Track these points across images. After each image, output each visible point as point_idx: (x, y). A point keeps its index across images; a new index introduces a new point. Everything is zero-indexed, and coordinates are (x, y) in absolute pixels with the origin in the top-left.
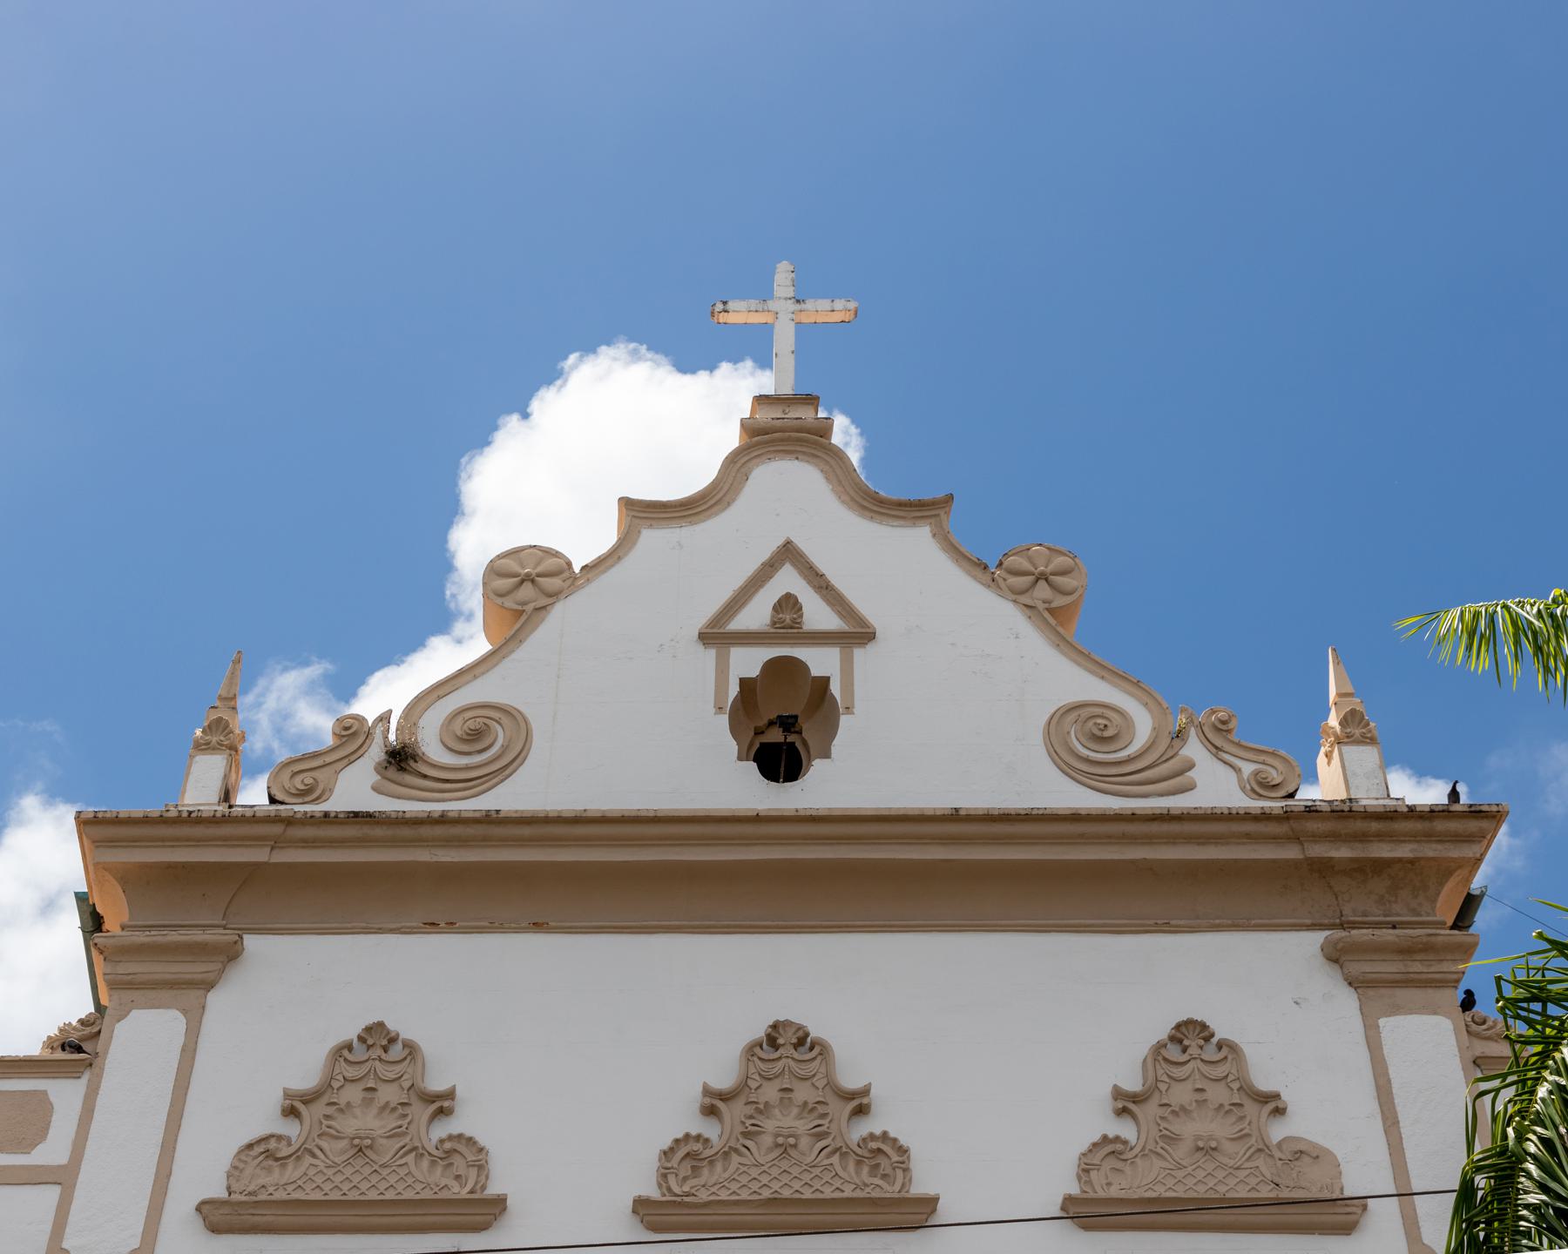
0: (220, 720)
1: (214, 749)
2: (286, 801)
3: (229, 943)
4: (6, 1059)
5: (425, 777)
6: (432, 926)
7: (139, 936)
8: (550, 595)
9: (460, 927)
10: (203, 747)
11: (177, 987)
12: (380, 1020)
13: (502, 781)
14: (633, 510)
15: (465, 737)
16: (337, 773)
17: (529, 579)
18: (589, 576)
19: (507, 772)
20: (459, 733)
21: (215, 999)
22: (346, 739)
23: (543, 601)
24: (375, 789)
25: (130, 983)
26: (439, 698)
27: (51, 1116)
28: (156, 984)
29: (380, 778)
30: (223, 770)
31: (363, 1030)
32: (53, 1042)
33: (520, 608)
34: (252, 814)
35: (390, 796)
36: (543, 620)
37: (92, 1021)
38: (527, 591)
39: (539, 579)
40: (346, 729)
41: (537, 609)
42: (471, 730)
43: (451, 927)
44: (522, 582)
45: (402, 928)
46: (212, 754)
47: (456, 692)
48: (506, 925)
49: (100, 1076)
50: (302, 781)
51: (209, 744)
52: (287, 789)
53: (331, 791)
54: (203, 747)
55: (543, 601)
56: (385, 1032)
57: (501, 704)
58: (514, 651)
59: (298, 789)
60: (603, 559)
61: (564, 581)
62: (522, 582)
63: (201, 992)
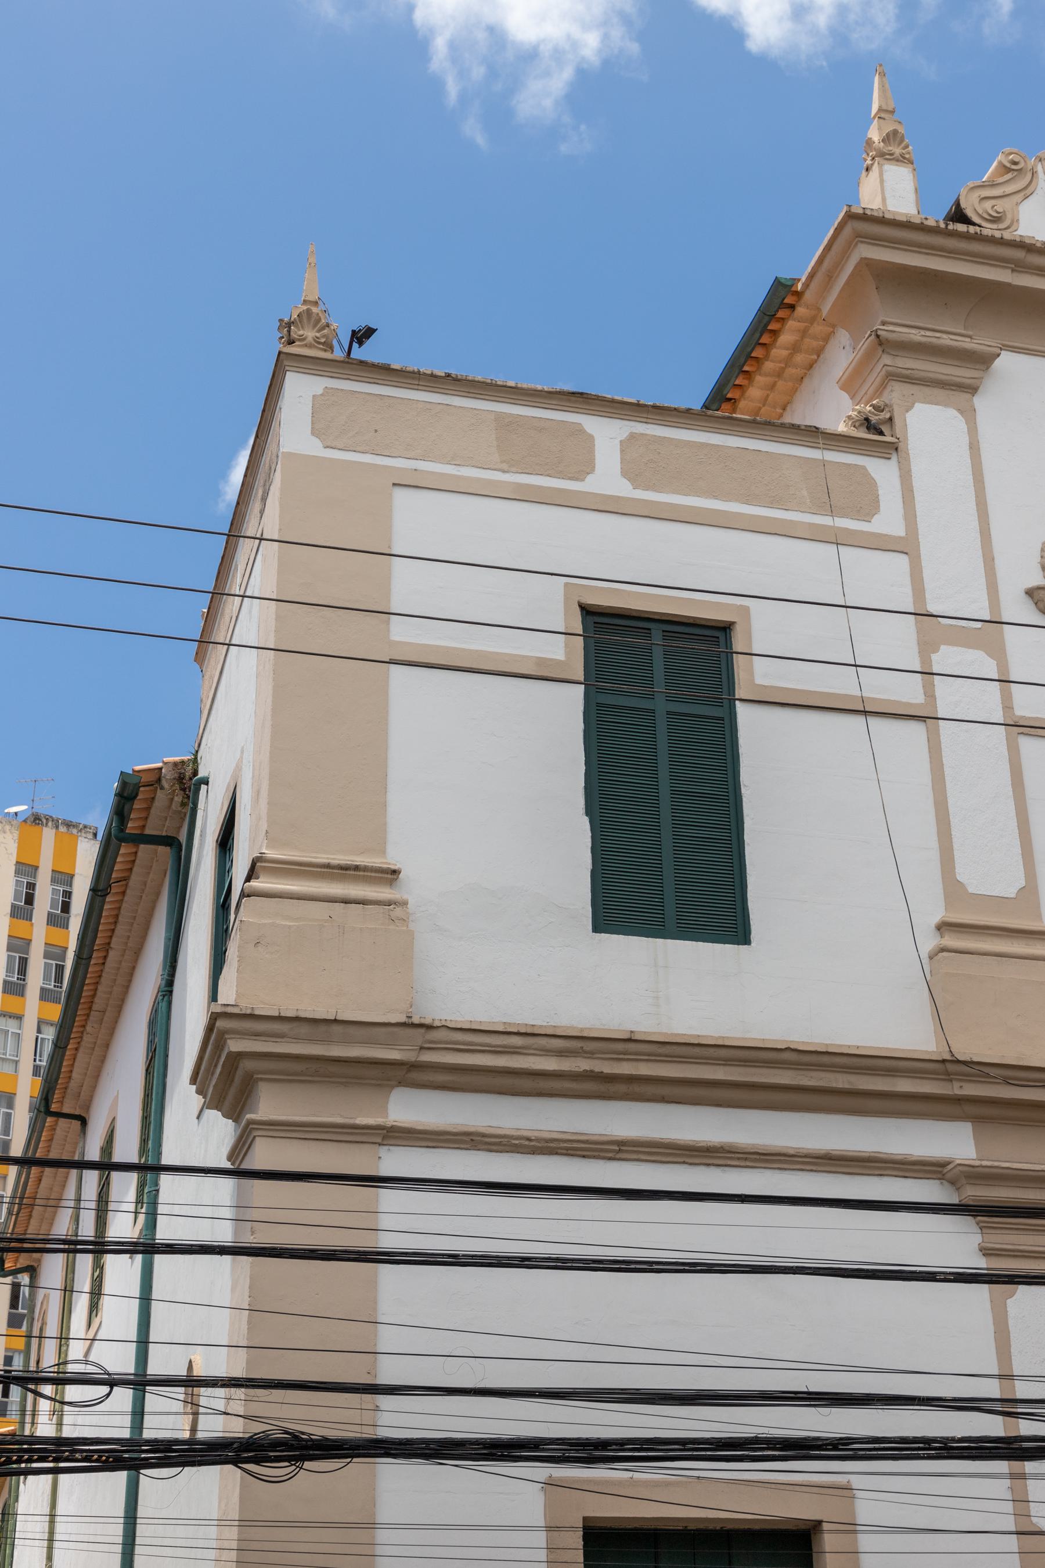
0: (895, 132)
1: (898, 160)
2: (982, 225)
3: (994, 354)
4: (828, 431)
10: (887, 157)
11: (948, 387)
16: (1018, 204)
21: (978, 401)
22: (1015, 173)
25: (907, 377)
28: (931, 382)
30: (913, 184)
34: (1000, 236)
37: (882, 407)
40: (1015, 163)
46: (897, 165)
49: (907, 459)
50: (993, 207)
51: (892, 154)
52: (981, 213)
53: (1018, 220)
54: (887, 157)
59: (990, 215)
63: (968, 396)
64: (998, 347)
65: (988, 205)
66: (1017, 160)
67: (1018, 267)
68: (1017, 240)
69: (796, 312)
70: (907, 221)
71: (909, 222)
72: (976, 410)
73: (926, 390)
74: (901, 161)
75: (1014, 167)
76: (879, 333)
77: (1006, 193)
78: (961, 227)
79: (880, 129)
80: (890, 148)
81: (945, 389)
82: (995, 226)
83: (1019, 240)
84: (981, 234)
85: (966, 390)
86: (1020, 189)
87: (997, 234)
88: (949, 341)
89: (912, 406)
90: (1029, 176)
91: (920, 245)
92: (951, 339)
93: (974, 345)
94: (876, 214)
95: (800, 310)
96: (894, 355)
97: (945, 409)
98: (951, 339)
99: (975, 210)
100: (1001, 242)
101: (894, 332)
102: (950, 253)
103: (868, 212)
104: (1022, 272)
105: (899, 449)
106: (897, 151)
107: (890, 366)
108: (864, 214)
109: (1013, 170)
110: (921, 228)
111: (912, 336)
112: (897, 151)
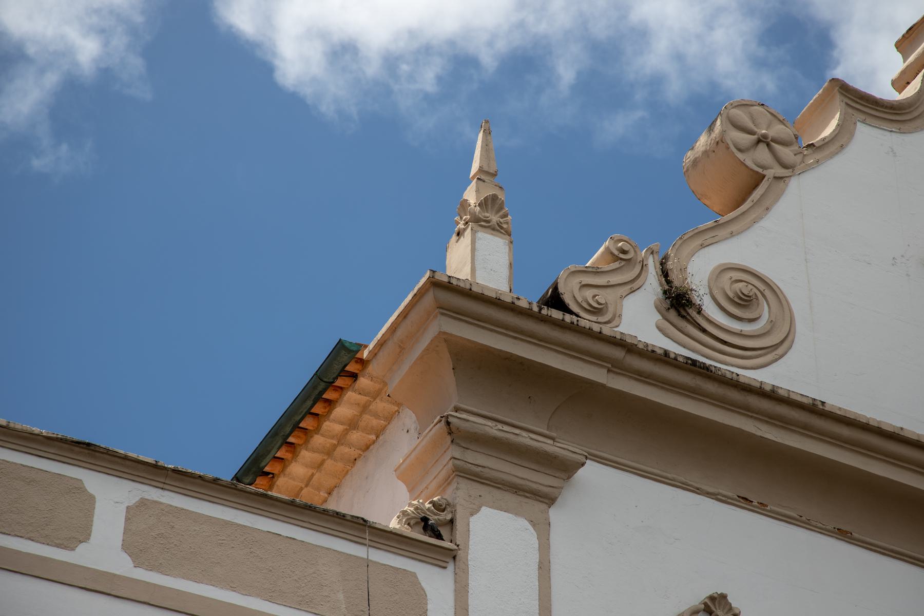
0: (494, 198)
1: (494, 229)
3: (578, 463)
4: (377, 526)
5: (704, 331)
6: (744, 502)
7: (492, 428)
8: (785, 166)
9: (770, 511)
10: (483, 223)
11: (521, 493)
12: (724, 592)
13: (776, 360)
14: (846, 96)
15: (737, 300)
17: (762, 140)
18: (818, 156)
19: (780, 351)
20: (731, 295)
21: (555, 514)
22: (623, 263)
23: (781, 172)
24: (660, 329)
25: (476, 475)
26: (703, 246)
27: (426, 604)
29: (661, 318)
31: (707, 597)
32: (410, 519)
33: (760, 170)
35: (674, 341)
36: (783, 192)
37: (444, 506)
38: (762, 153)
39: (773, 144)
40: (624, 252)
41: (775, 178)
42: (743, 294)
43: (762, 509)
44: (759, 141)
45: (718, 494)
46: (492, 234)
47: (715, 245)
48: (814, 523)
50: (594, 296)
52: (580, 301)
53: (620, 316)
54: (483, 223)
55: (781, 172)
56: (728, 607)
57: (761, 274)
58: (763, 218)
59: (590, 305)
60: (827, 143)
61: (795, 155)
62: (759, 141)
63: (544, 506)
64: (584, 455)
65: (589, 293)
66: (626, 249)
67: (616, 368)
68: (617, 337)
69: (358, 382)
70: (496, 298)
71: (499, 299)
72: (551, 524)
73: (497, 494)
74: (498, 231)
75: (622, 256)
76: (451, 419)
77: (610, 284)
78: (556, 314)
79: (477, 191)
80: (487, 215)
81: (518, 495)
82: (594, 318)
83: (619, 338)
84: (578, 325)
85: (542, 500)
86: (626, 281)
87: (596, 328)
88: (528, 440)
89: (478, 510)
90: (637, 269)
91: (507, 327)
92: (532, 439)
93: (556, 448)
94: (462, 285)
95: (363, 382)
96: (464, 447)
97: (515, 518)
98: (532, 439)
99: (574, 297)
100: (599, 337)
101: (468, 421)
102: (540, 340)
103: (454, 282)
104: (619, 374)
105: (457, 558)
106: (495, 219)
107: (459, 459)
108: (449, 282)
109: (621, 259)
110: (512, 308)
111: (487, 429)
112: (495, 219)
